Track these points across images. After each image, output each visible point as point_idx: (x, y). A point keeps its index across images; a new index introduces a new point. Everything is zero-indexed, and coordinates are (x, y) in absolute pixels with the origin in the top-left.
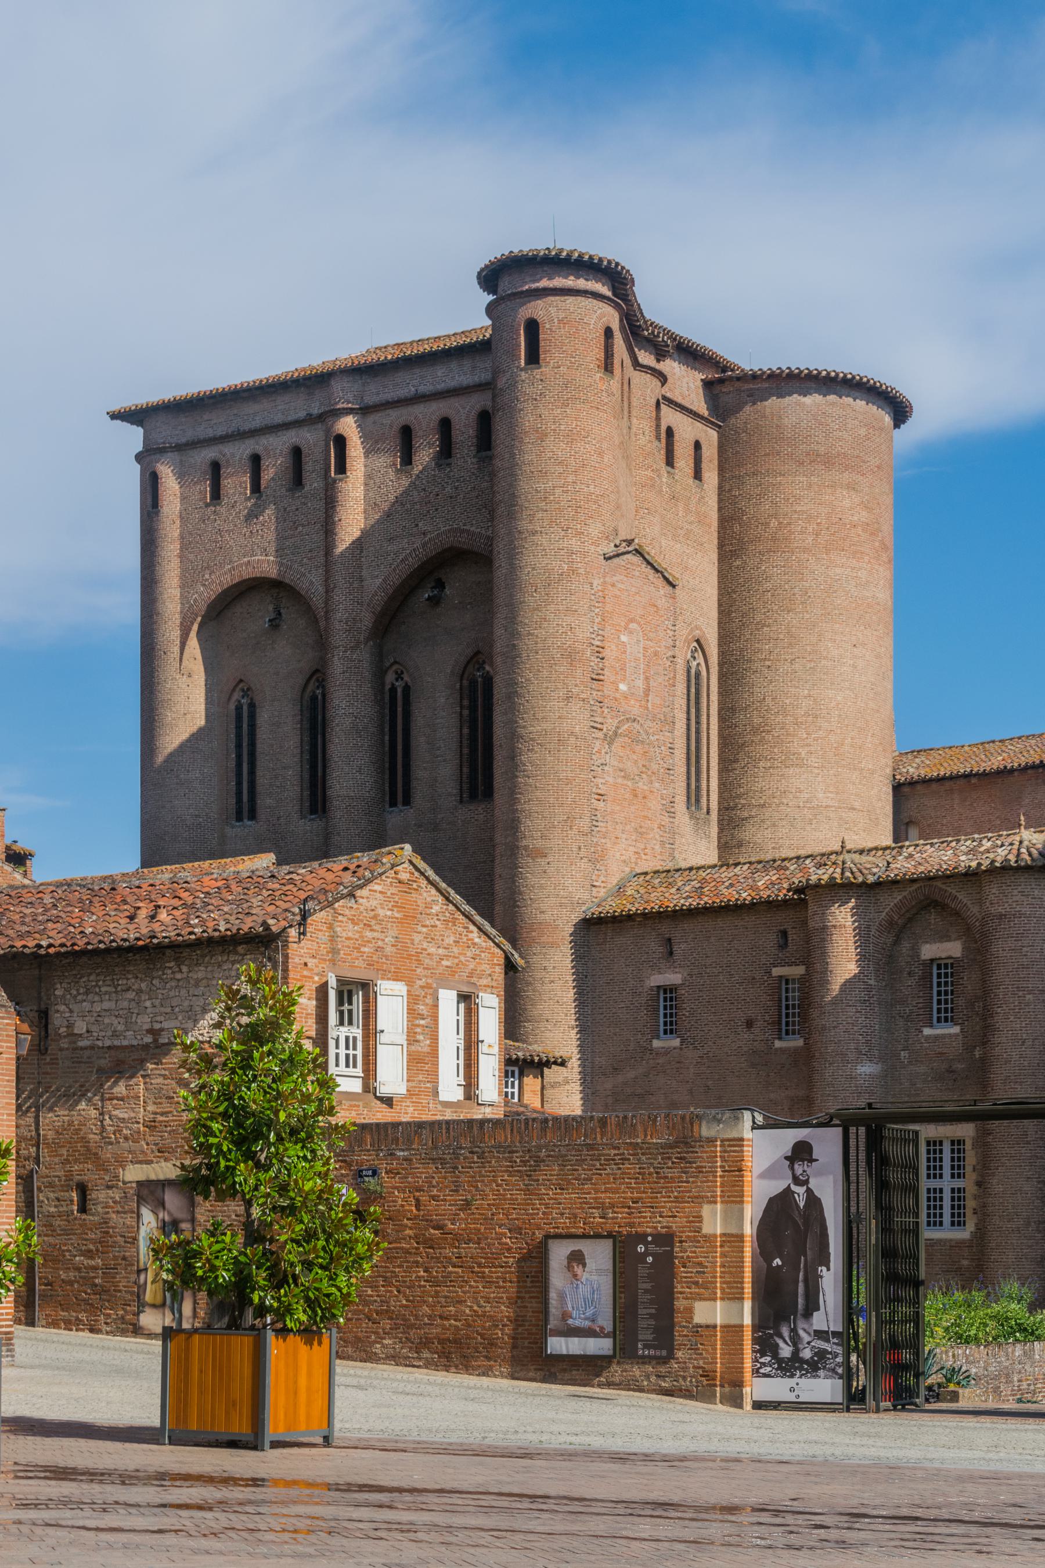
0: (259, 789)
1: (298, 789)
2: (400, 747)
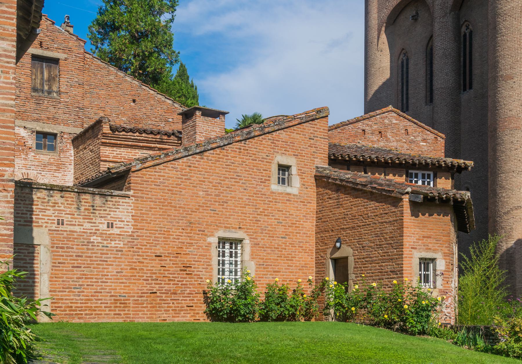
0: (410, 96)
1: (424, 92)
2: (468, 62)
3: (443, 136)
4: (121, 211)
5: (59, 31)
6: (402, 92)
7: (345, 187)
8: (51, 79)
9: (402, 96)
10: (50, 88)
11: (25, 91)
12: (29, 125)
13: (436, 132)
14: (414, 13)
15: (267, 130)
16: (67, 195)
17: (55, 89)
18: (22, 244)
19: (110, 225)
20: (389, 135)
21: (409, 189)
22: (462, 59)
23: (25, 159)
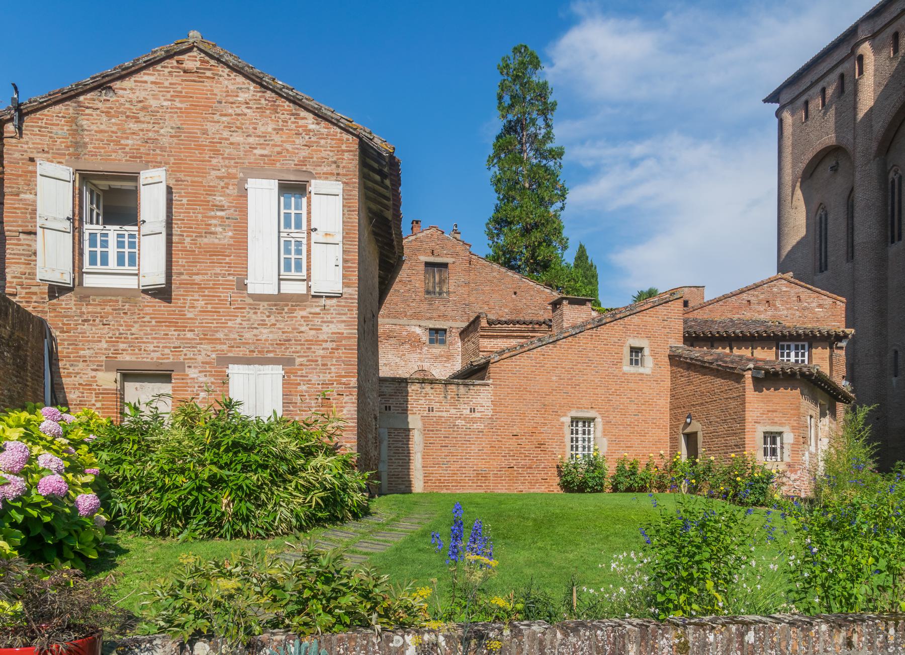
0: (829, 254)
3: (844, 299)
4: (482, 398)
5: (448, 239)
6: (821, 250)
7: (695, 365)
8: (442, 282)
9: (821, 254)
10: (441, 289)
11: (420, 294)
12: (423, 323)
13: (835, 296)
14: (834, 163)
15: (618, 316)
16: (436, 386)
17: (445, 290)
18: (400, 429)
19: (473, 410)
20: (778, 304)
21: (751, 366)
22: (890, 208)
23: (420, 353)
